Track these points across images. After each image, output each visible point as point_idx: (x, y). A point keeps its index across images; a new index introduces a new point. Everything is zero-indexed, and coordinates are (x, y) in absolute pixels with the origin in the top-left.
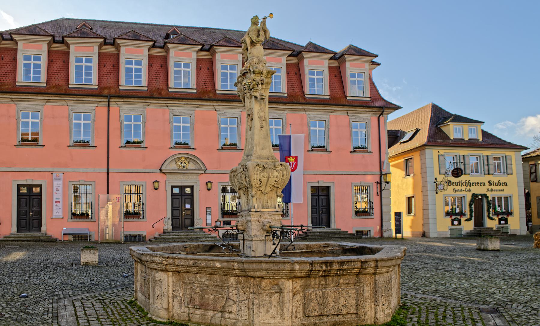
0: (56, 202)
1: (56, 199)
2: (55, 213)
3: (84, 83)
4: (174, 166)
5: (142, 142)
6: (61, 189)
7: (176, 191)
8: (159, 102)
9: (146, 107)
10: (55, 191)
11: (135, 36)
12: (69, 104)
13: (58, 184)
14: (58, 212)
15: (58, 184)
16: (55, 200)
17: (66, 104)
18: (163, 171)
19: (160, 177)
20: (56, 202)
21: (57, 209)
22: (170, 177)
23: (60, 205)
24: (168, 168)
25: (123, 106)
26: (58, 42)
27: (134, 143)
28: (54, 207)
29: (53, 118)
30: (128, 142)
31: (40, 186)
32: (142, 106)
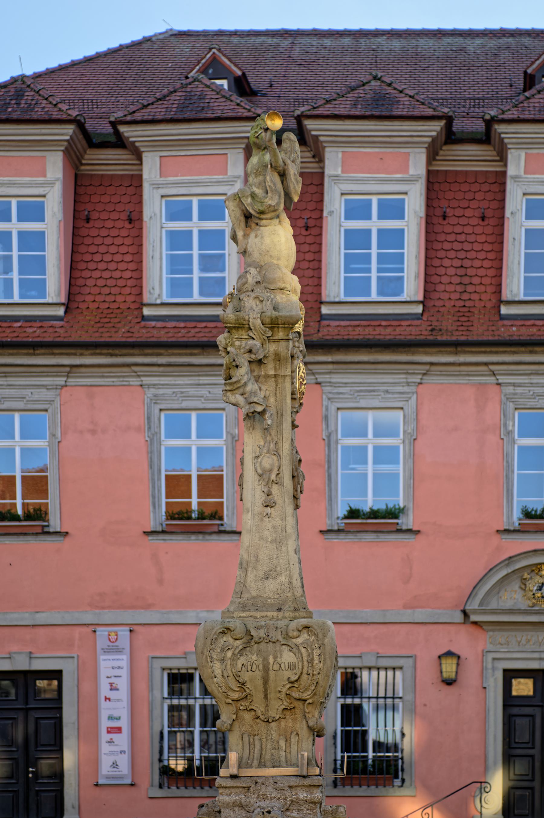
0: (110, 730)
1: (110, 718)
2: (105, 769)
3: (196, 297)
4: (513, 597)
5: (402, 511)
6: (123, 684)
7: (523, 687)
8: (462, 358)
9: (417, 379)
10: (104, 690)
11: (379, 99)
12: (147, 380)
13: (113, 669)
14: (115, 765)
15: (113, 669)
16: (105, 723)
17: (135, 381)
18: (473, 618)
19: (463, 641)
20: (110, 730)
21: (112, 753)
22: (501, 636)
23: (122, 741)
24: (493, 605)
25: (336, 378)
26: (104, 145)
27: (374, 514)
28: (105, 748)
29: (93, 432)
30: (353, 514)
31: (57, 675)
32: (401, 378)
